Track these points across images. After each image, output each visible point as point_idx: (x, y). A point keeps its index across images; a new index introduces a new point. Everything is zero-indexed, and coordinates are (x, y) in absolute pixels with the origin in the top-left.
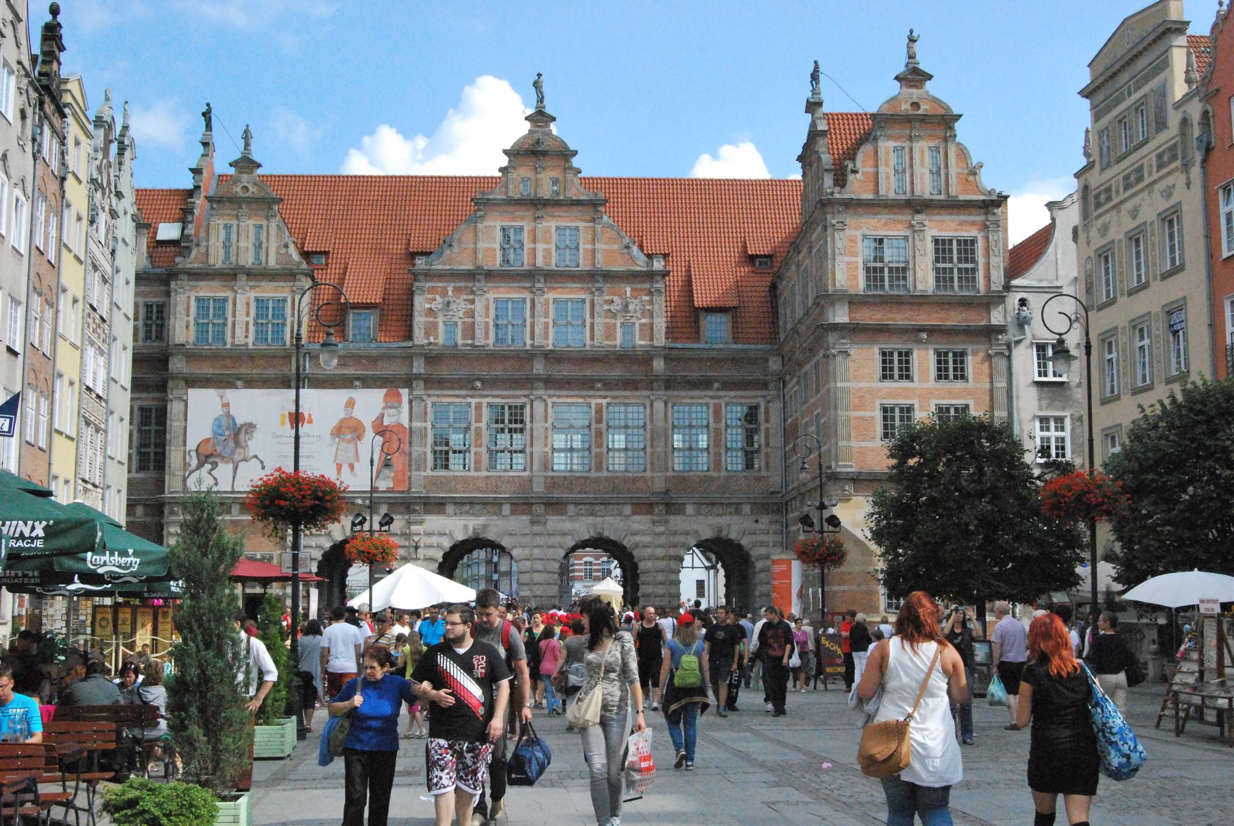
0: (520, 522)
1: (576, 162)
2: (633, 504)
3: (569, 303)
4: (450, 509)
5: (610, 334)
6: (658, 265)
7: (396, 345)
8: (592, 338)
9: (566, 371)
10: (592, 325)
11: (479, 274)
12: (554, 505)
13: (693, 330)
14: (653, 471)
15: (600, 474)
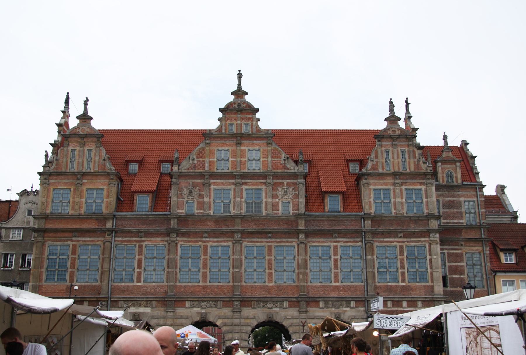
0: (227, 311)
1: (258, 115)
2: (289, 301)
3: (254, 191)
4: (188, 304)
5: (275, 207)
6: (304, 168)
7: (161, 213)
8: (266, 209)
9: (253, 227)
10: (266, 202)
11: (207, 175)
12: (246, 302)
13: (322, 204)
14: (299, 283)
15: (271, 285)
